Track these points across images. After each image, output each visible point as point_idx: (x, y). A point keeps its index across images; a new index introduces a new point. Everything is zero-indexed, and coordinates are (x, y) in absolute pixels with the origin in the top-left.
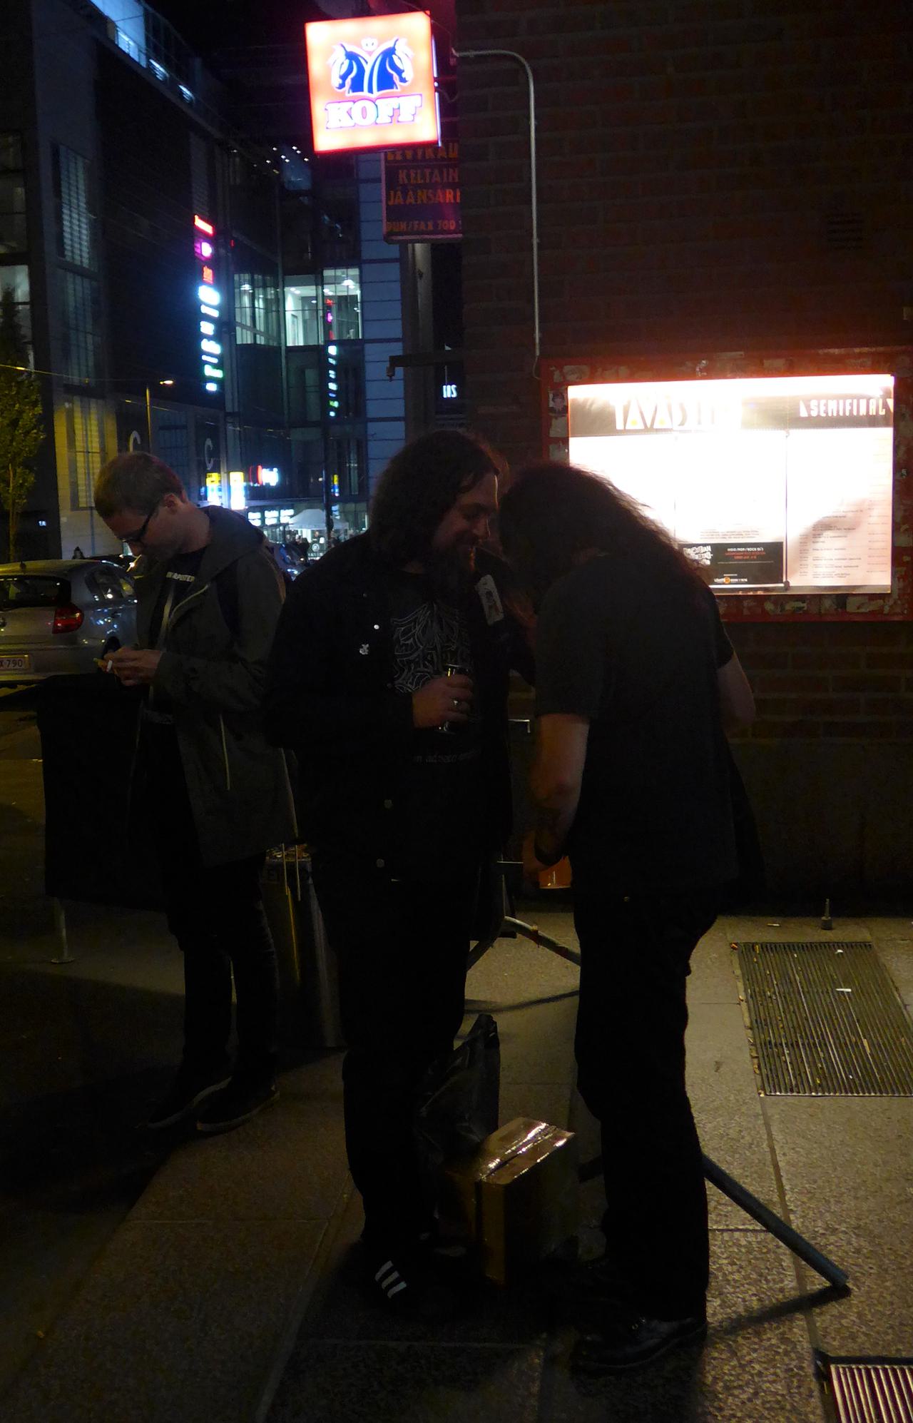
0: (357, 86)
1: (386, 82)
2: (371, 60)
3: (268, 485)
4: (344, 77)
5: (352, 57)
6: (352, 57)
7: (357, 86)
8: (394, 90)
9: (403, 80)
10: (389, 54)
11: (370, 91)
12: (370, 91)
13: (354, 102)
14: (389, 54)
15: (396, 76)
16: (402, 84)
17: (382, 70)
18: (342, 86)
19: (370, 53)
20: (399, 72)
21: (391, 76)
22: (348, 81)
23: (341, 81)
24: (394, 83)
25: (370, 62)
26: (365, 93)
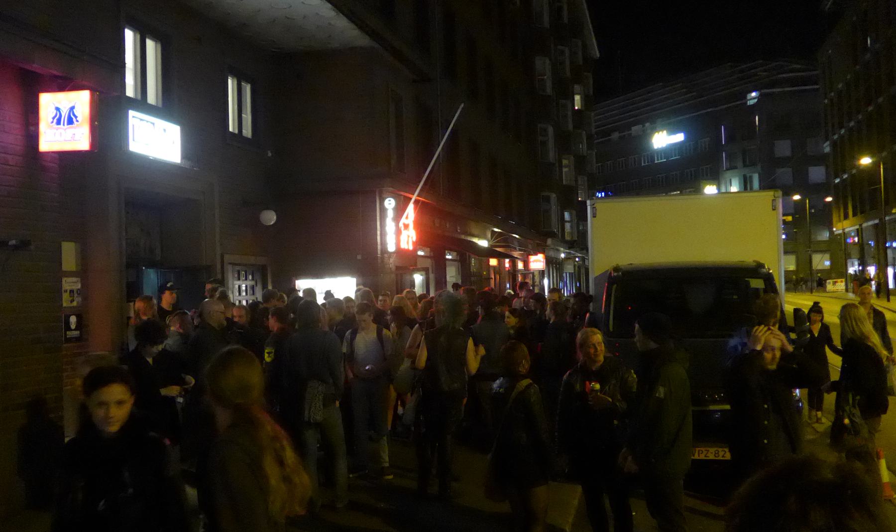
0: (58, 123)
1: (70, 122)
2: (65, 111)
3: (348, 299)
4: (54, 118)
5: (58, 109)
6: (58, 109)
7: (58, 123)
8: (73, 125)
9: (77, 121)
10: (72, 108)
11: (64, 125)
12: (64, 125)
13: (57, 130)
14: (72, 108)
15: (74, 120)
16: (77, 123)
17: (69, 116)
18: (52, 122)
19: (65, 108)
20: (76, 117)
21: (72, 119)
22: (55, 120)
23: (52, 120)
24: (73, 122)
25: (65, 113)
26: (62, 125)
